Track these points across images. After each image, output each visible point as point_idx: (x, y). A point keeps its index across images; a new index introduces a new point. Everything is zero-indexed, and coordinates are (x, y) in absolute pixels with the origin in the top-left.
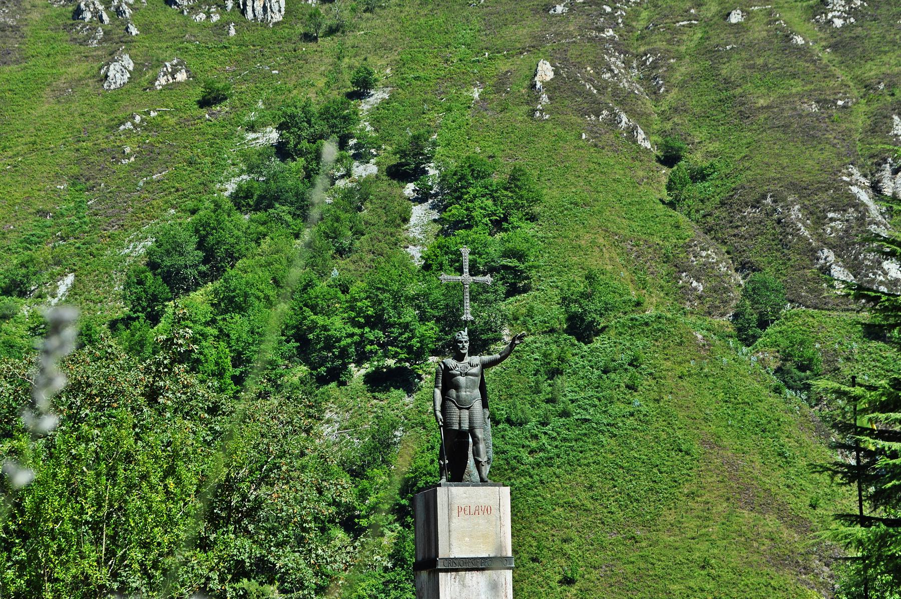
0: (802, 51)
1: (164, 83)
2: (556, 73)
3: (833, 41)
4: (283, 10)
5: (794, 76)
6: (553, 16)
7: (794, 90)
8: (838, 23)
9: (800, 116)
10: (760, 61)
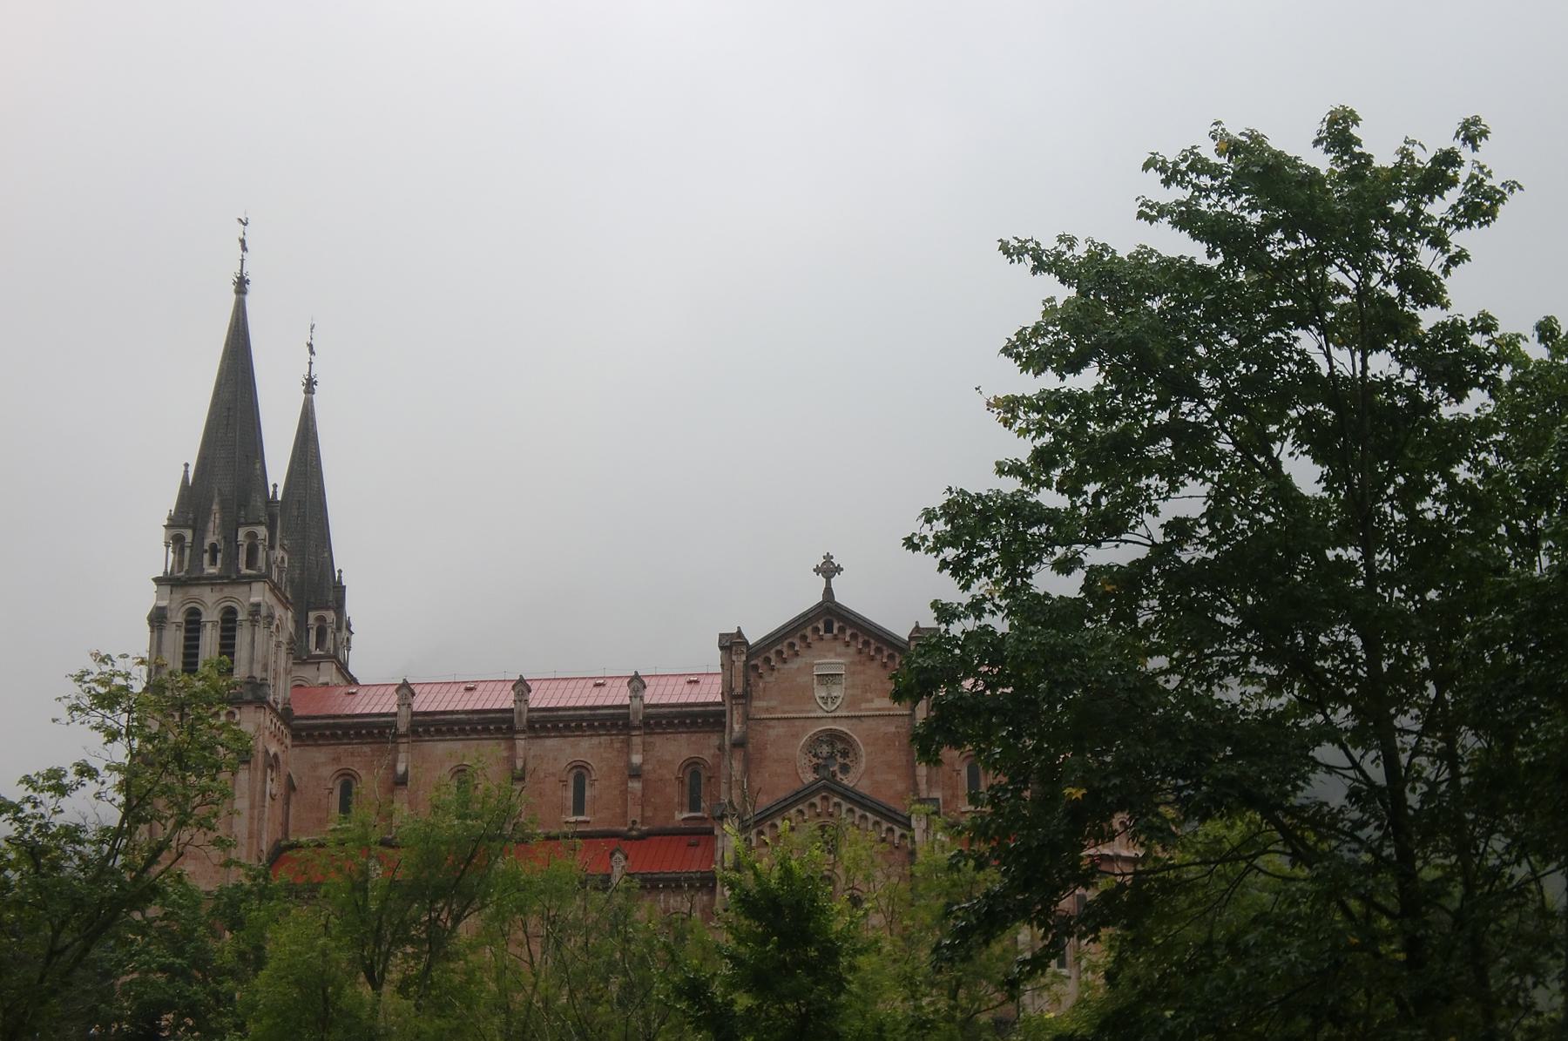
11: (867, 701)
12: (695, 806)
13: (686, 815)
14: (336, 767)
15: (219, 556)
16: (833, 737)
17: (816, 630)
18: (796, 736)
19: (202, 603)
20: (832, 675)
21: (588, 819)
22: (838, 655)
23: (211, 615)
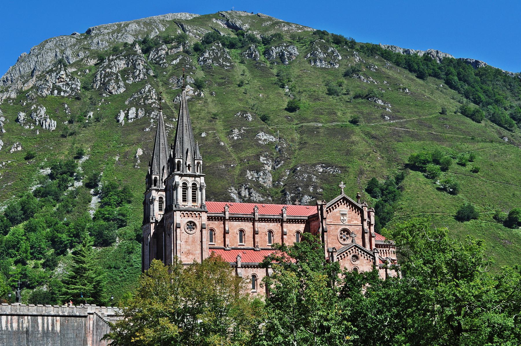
0: (223, 148)
1: (14, 151)
2: (143, 152)
3: (233, 144)
4: (55, 126)
5: (219, 156)
6: (145, 132)
7: (218, 161)
8: (236, 138)
9: (219, 170)
10: (209, 150)
15: (191, 168)
16: (344, 230)
17: (340, 202)
18: (337, 229)
23: (190, 185)
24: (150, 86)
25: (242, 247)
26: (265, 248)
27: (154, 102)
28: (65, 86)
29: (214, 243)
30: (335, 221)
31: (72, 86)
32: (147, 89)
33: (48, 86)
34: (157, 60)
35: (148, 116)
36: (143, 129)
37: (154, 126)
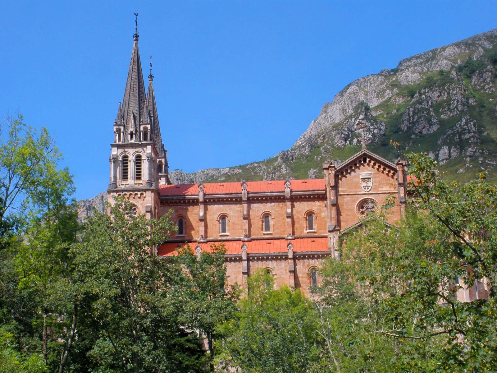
6: (459, 173)
11: (381, 188)
12: (311, 227)
13: (308, 231)
14: (177, 214)
15: (134, 136)
18: (355, 201)
19: (129, 153)
20: (367, 178)
21: (272, 232)
22: (369, 171)
23: (132, 158)
24: (468, 117)
25: (224, 238)
26: (259, 237)
27: (473, 137)
28: (365, 133)
29: (184, 235)
30: (352, 189)
31: (375, 131)
32: (464, 121)
33: (345, 135)
34: (482, 85)
35: (464, 154)
36: (456, 171)
37: (471, 165)
